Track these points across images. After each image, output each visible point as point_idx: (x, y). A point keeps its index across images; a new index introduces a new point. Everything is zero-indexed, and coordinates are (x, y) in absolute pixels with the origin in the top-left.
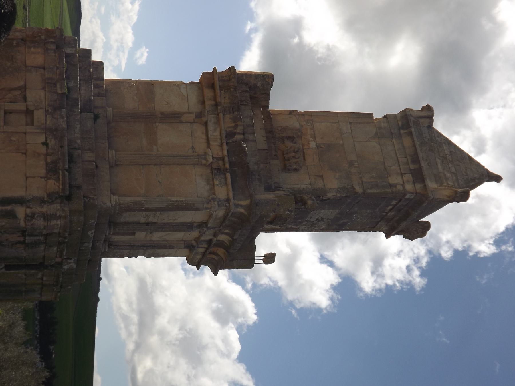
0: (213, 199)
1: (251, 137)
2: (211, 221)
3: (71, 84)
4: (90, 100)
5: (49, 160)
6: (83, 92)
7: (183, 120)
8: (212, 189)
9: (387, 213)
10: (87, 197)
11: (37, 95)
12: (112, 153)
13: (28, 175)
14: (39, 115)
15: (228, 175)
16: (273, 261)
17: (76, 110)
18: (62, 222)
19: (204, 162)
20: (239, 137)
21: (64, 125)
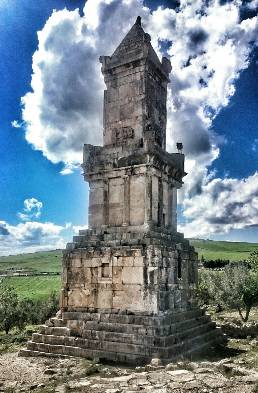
0: (146, 174)
1: (116, 155)
2: (158, 175)
3: (90, 245)
4: (98, 236)
5: (126, 255)
6: (94, 240)
7: (108, 190)
8: (142, 174)
9: (157, 81)
10: (144, 237)
11: (95, 262)
12: (124, 225)
13: (133, 265)
14: (104, 260)
15: (135, 166)
17: (102, 243)
18: (156, 248)
19: (128, 179)
20: (116, 162)
21: (109, 248)
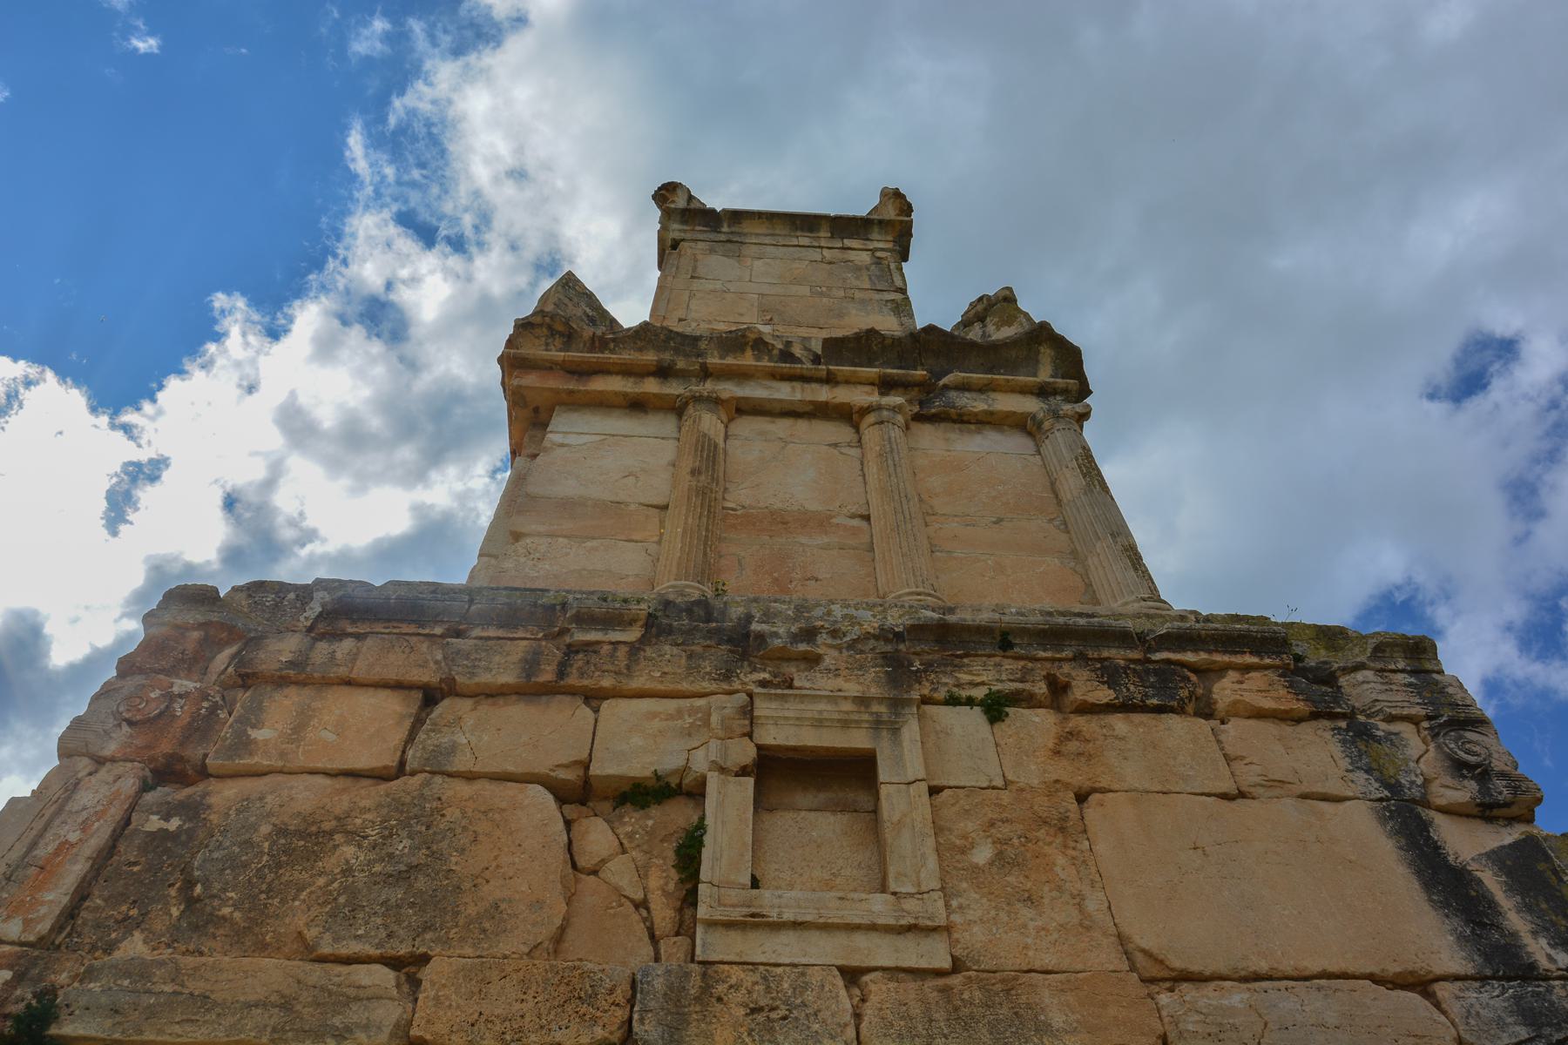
5: (1104, 695)
14: (788, 726)
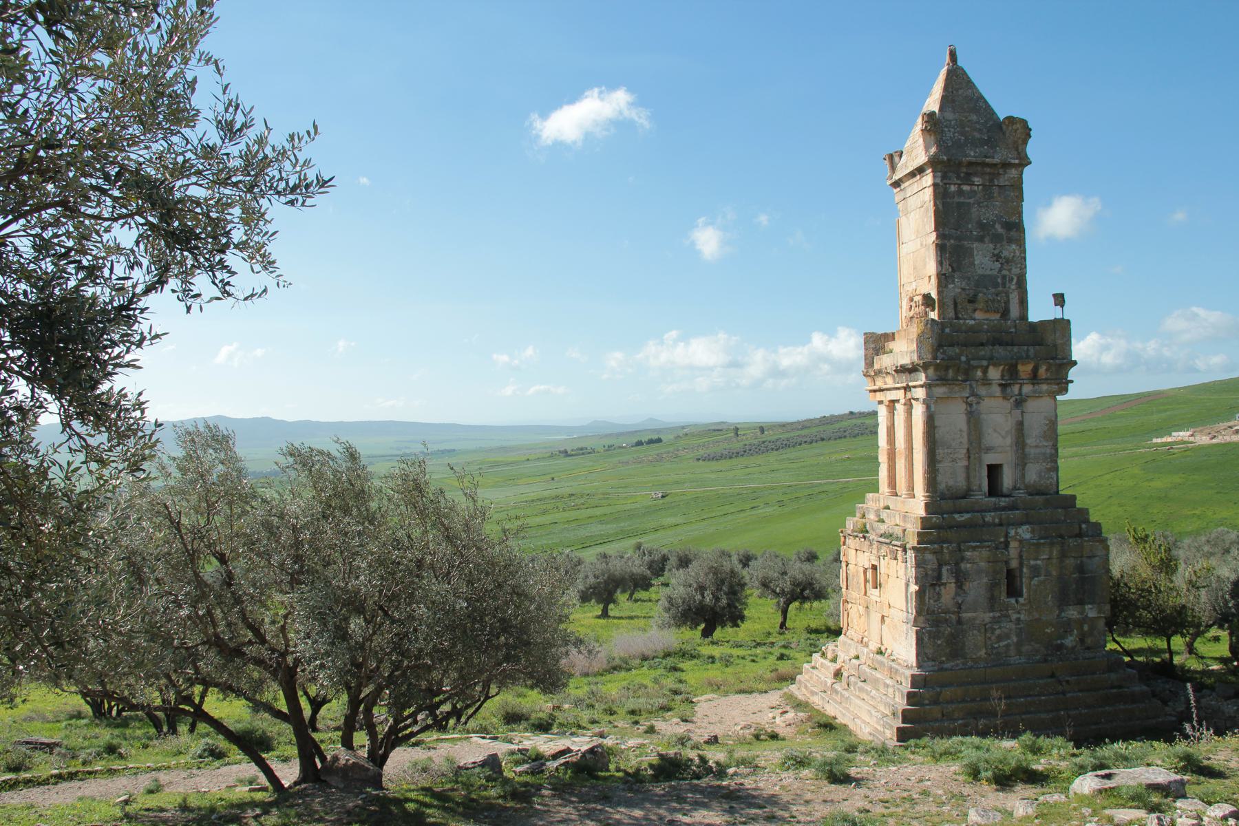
16: (1062, 295)
